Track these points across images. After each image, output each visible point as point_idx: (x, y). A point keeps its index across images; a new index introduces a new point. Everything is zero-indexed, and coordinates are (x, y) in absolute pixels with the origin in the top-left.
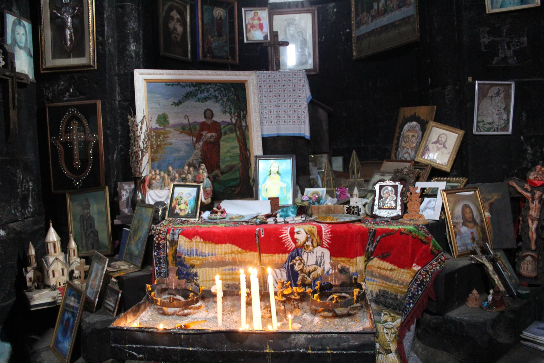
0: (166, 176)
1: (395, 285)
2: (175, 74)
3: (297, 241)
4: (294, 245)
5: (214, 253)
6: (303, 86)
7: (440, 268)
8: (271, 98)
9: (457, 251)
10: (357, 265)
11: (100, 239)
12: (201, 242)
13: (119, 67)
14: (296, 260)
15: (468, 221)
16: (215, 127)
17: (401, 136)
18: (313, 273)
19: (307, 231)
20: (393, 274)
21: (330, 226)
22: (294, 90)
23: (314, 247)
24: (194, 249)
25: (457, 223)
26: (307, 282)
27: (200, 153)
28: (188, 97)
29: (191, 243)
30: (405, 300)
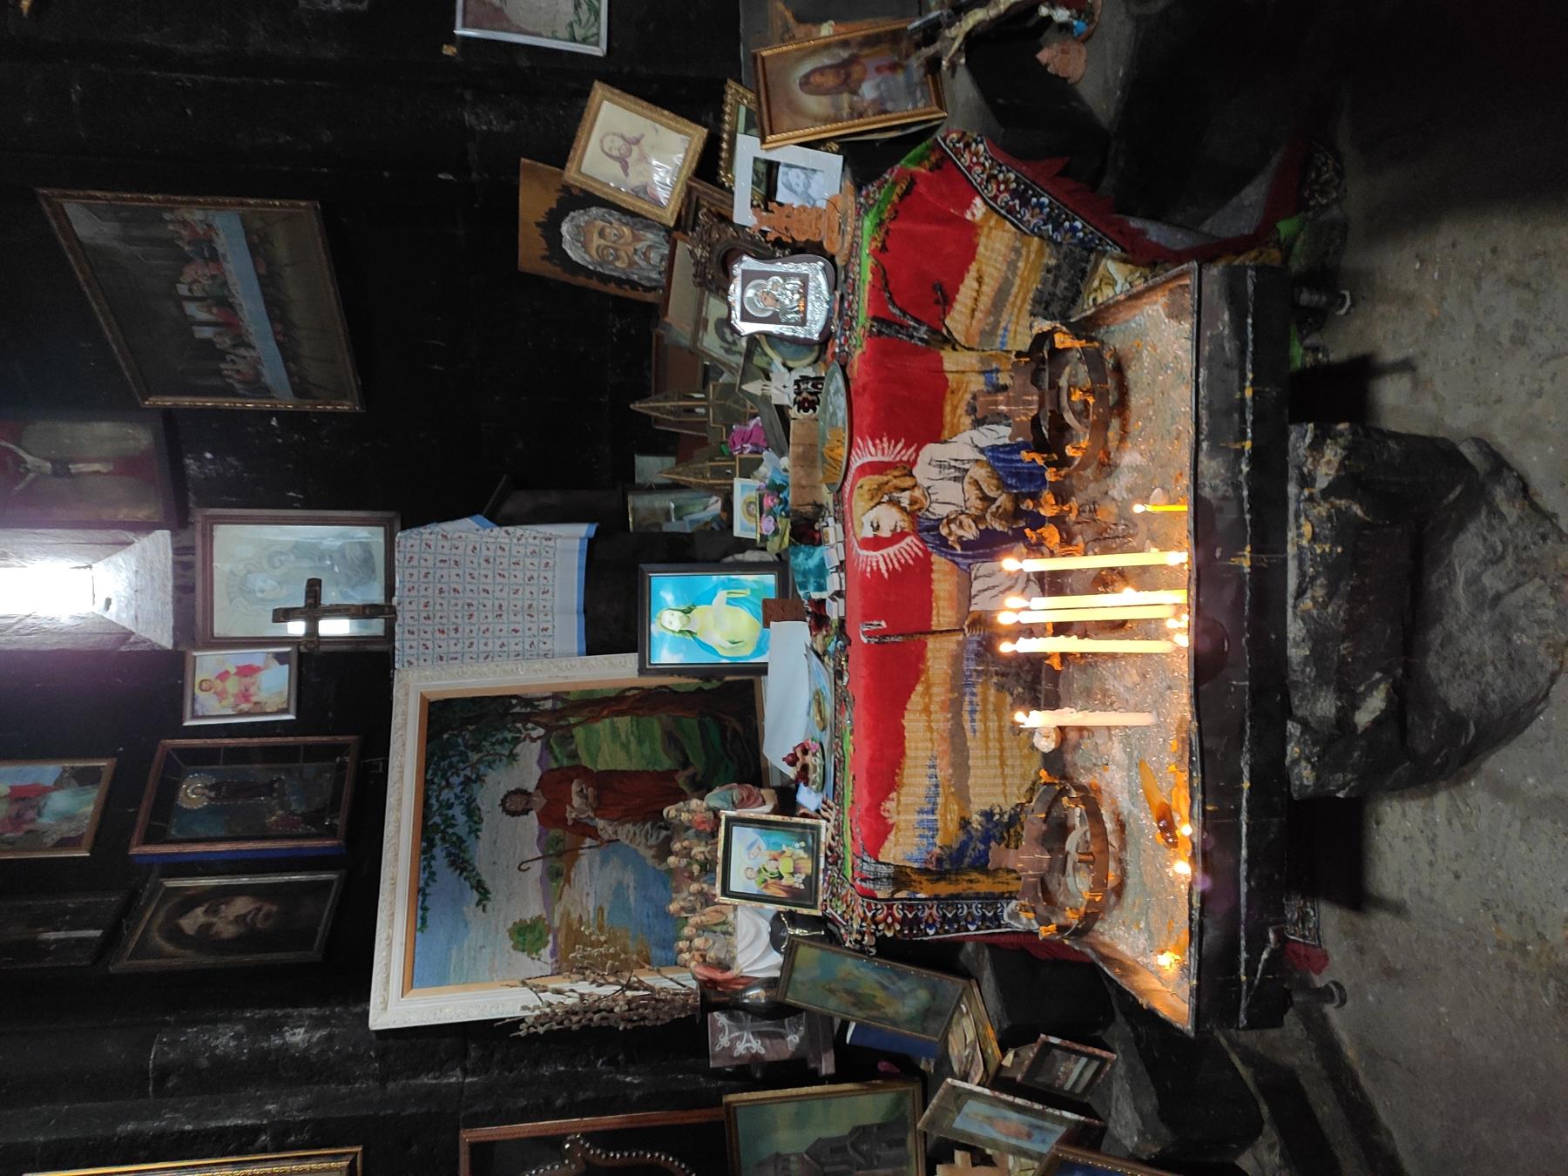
0: (695, 919)
1: (1019, 272)
2: (392, 904)
3: (899, 530)
4: (908, 540)
5: (928, 763)
6: (445, 537)
7: (982, 142)
8: (475, 628)
9: (928, 109)
10: (963, 372)
11: (877, 1120)
13: (356, 1079)
14: (950, 533)
15: (845, 76)
16: (555, 782)
17: (599, 269)
18: (986, 490)
19: (872, 504)
20: (991, 275)
22: (456, 562)
23: (915, 485)
25: (851, 107)
26: (1009, 506)
27: (629, 826)
28: (464, 861)
29: (902, 825)
30: (1061, 244)
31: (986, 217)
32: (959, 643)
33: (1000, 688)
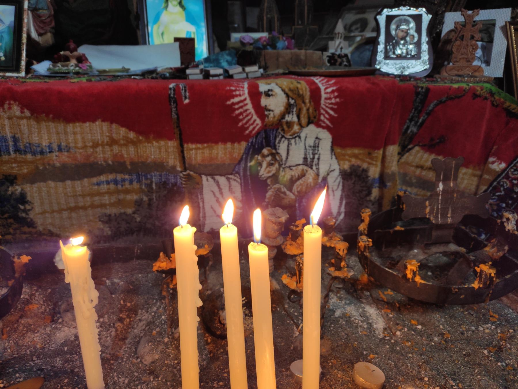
3: (266, 113)
4: (258, 121)
5: (63, 144)
12: (26, 117)
14: (264, 156)
18: (298, 183)
19: (287, 90)
21: (333, 81)
24: (9, 135)
31: (491, 172)
32: (174, 167)
33: (139, 203)
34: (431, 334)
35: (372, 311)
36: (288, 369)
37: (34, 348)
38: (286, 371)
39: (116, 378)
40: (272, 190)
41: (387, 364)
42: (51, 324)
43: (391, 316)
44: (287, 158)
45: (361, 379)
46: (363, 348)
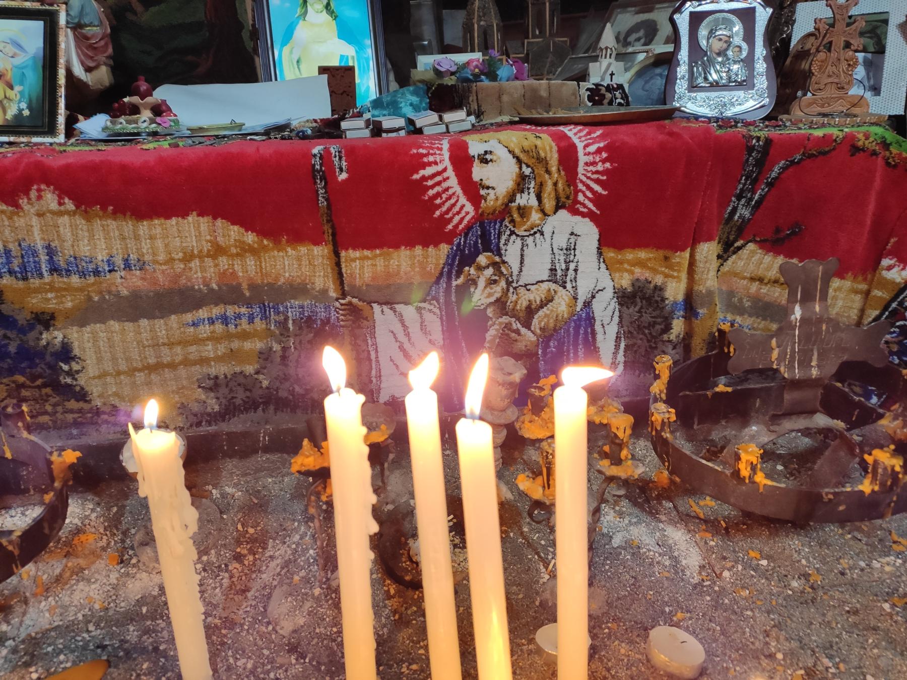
3: (482, 192)
4: (469, 208)
5: (133, 257)
12: (67, 213)
14: (480, 268)
18: (541, 313)
19: (517, 151)
21: (598, 133)
23: (546, 215)
24: (39, 245)
29: (20, 222)
31: (885, 284)
32: (324, 292)
33: (265, 356)
34: (786, 576)
35: (677, 535)
36: (531, 641)
37: (90, 609)
38: (528, 644)
39: (231, 660)
40: (496, 327)
41: (709, 630)
42: (118, 567)
43: (712, 543)
44: (521, 271)
45: (662, 656)
46: (664, 602)
